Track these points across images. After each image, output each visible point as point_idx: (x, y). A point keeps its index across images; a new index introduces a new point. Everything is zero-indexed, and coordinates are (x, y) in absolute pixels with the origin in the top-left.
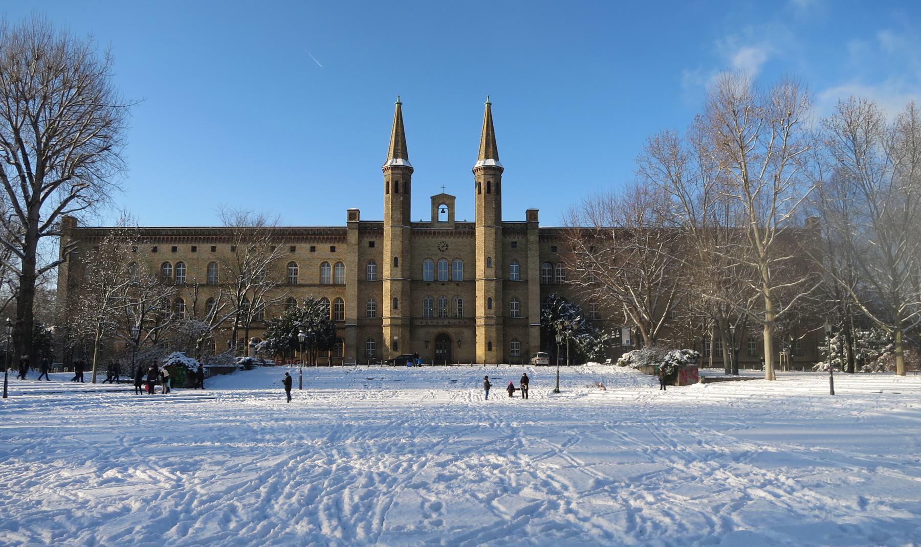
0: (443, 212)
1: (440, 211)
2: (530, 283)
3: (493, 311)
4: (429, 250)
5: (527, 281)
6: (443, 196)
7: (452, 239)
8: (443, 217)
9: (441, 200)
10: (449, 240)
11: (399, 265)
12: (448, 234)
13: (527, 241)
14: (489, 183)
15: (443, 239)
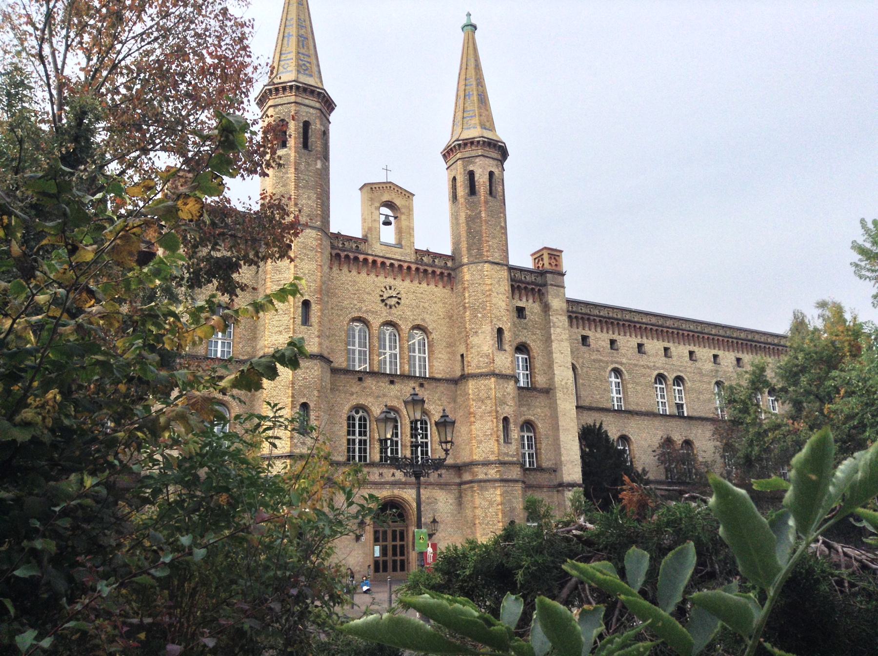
0: (387, 223)
1: (382, 218)
2: (559, 395)
3: (513, 448)
4: (362, 301)
5: (548, 392)
6: (389, 186)
7: (407, 283)
8: (388, 235)
9: (389, 199)
10: (403, 285)
11: (314, 319)
12: (398, 269)
13: (546, 308)
14: (491, 174)
15: (390, 281)
